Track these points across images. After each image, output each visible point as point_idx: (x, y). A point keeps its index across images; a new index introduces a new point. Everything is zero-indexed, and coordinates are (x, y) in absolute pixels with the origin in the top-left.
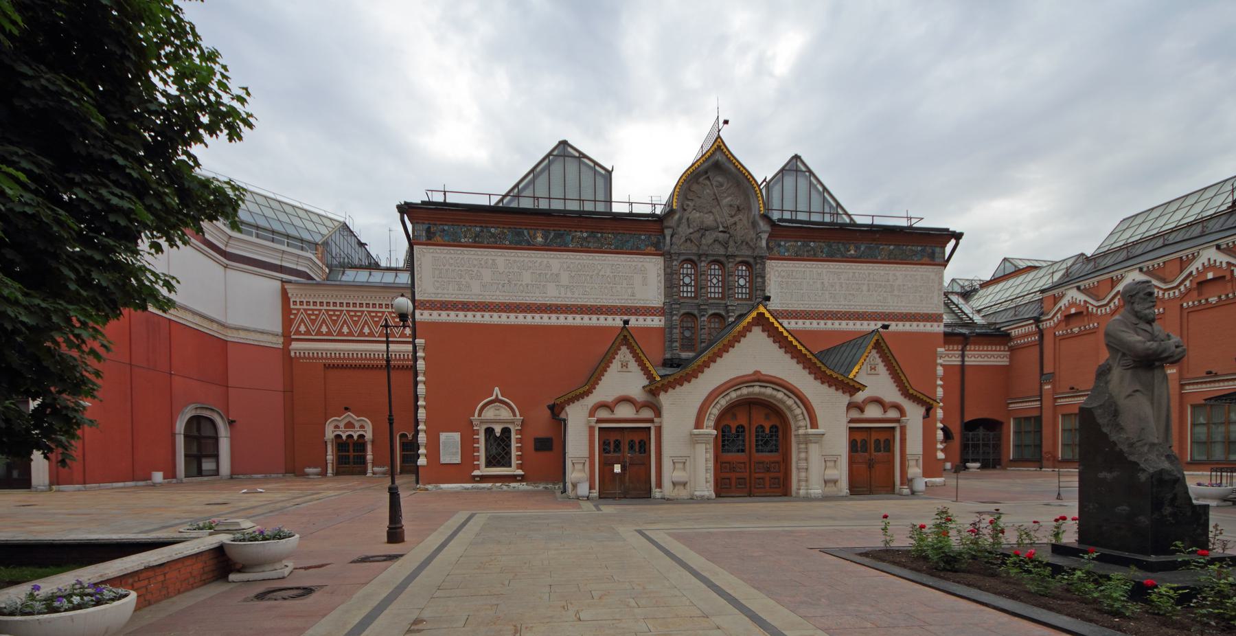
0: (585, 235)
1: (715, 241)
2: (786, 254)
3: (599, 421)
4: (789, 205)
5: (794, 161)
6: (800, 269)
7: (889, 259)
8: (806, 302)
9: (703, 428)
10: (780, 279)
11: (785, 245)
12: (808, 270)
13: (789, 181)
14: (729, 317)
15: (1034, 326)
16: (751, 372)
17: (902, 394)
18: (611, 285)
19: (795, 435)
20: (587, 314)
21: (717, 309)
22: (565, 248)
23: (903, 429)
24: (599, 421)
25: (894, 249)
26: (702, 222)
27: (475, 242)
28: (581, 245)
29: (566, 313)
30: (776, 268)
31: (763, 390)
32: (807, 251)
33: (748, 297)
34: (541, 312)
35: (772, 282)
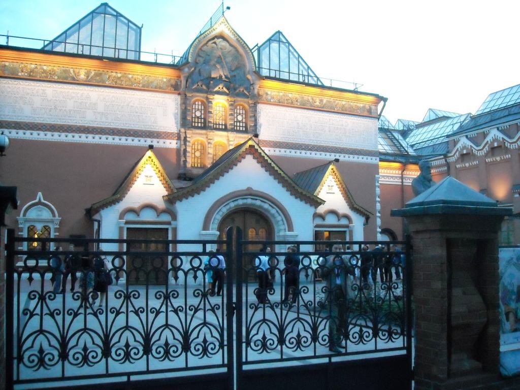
0: (119, 75)
3: (127, 223)
4: (274, 66)
9: (209, 230)
13: (275, 45)
15: (444, 160)
16: (245, 188)
17: (350, 208)
18: (139, 114)
19: (278, 236)
20: (117, 135)
22: (103, 84)
28: (116, 82)
29: (101, 134)
31: (254, 202)
33: (244, 129)
34: (80, 133)
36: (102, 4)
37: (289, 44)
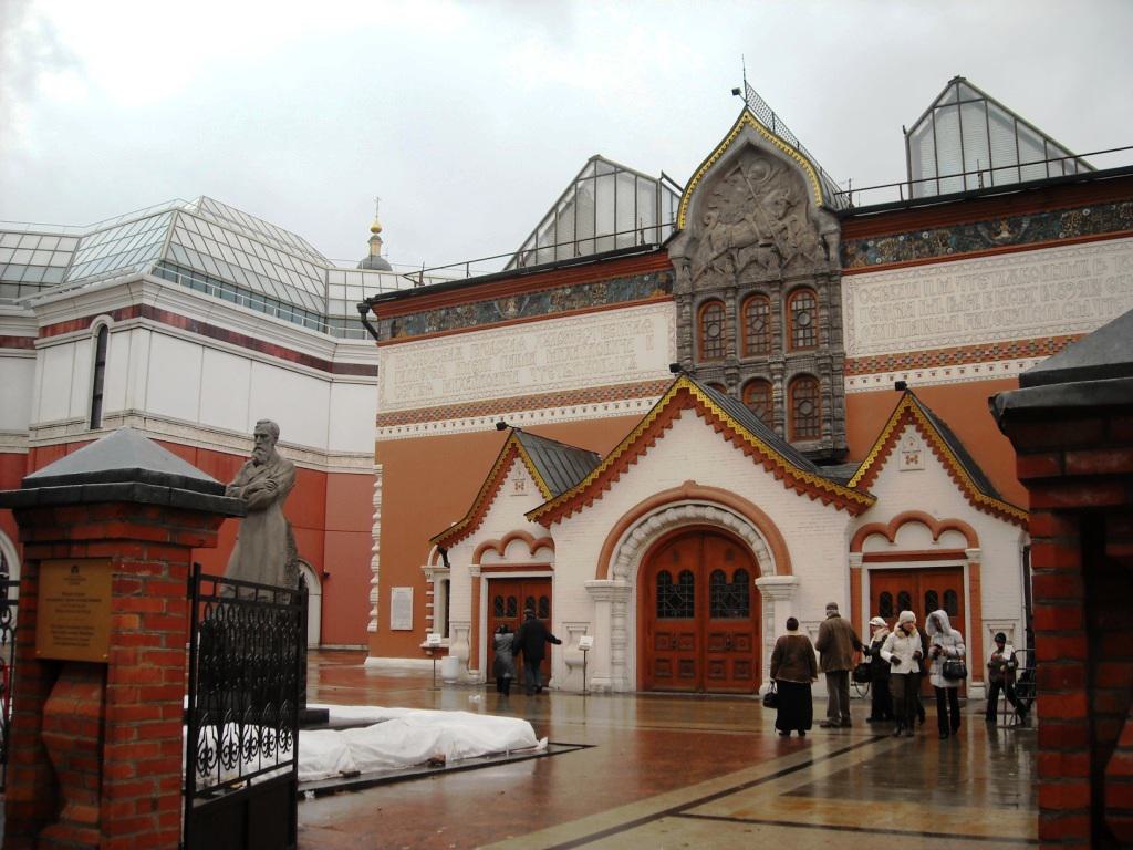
1: (751, 262)
2: (878, 260)
5: (954, 87)
6: (906, 281)
7: (1083, 234)
8: (920, 337)
10: (870, 304)
11: (875, 246)
12: (921, 280)
13: (948, 121)
14: (775, 381)
16: (680, 483)
17: (972, 504)
18: (603, 357)
21: (757, 371)
23: (975, 568)
24: (484, 569)
25: (1090, 215)
26: (730, 239)
27: (440, 329)
30: (863, 287)
32: (918, 248)
33: (814, 343)
35: (857, 313)
36: (591, 160)
37: (986, 98)
